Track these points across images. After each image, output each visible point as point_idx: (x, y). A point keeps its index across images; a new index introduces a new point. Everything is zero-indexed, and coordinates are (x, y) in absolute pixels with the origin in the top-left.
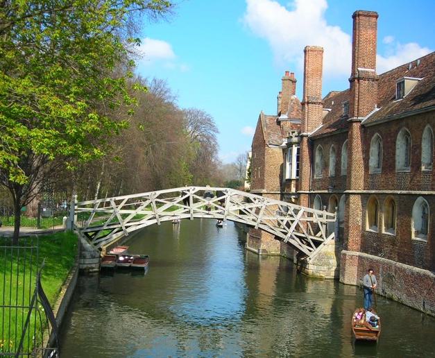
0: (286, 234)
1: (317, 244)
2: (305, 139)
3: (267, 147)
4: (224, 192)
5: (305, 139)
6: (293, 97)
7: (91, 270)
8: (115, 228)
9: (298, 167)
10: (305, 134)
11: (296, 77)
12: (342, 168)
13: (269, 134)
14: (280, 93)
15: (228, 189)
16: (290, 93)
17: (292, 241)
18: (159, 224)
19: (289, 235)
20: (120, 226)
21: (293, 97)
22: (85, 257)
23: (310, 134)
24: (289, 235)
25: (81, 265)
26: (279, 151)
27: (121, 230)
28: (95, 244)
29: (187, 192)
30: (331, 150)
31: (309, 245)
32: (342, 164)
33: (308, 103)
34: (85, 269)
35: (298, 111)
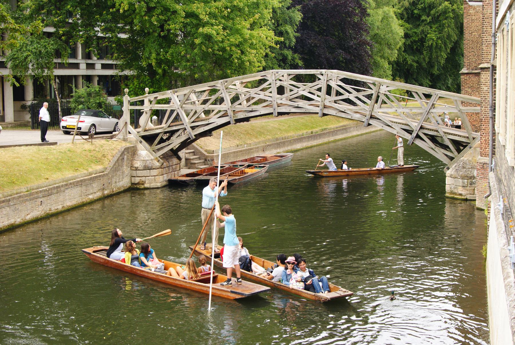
0: (410, 132)
4: (320, 77)
7: (147, 185)
8: (177, 130)
15: (323, 71)
17: (418, 142)
22: (137, 169)
24: (414, 134)
25: (133, 178)
34: (138, 184)
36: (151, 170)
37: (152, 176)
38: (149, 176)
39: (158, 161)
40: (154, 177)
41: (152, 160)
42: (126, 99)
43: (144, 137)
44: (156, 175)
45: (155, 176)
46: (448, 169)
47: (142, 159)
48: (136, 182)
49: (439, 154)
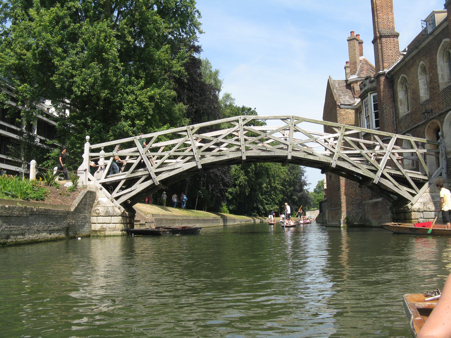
0: (375, 172)
1: (420, 184)
2: (383, 79)
3: (338, 108)
5: (383, 79)
6: (361, 58)
7: (107, 233)
9: (377, 116)
10: (381, 72)
11: (361, 38)
12: (440, 81)
13: (340, 96)
14: (347, 62)
16: (357, 52)
18: (200, 167)
19: (379, 174)
20: (147, 172)
21: (361, 58)
23: (386, 71)
24: (379, 174)
26: (352, 113)
27: (149, 177)
28: (117, 198)
29: (236, 124)
30: (419, 70)
31: (409, 186)
32: (440, 77)
33: (381, 37)
35: (367, 70)
36: (113, 217)
37: (113, 223)
38: (110, 223)
39: (119, 208)
40: (115, 224)
41: (113, 206)
42: (87, 146)
43: (104, 185)
44: (117, 222)
45: (116, 223)
46: (412, 205)
47: (104, 205)
48: (97, 229)
49: (403, 191)
